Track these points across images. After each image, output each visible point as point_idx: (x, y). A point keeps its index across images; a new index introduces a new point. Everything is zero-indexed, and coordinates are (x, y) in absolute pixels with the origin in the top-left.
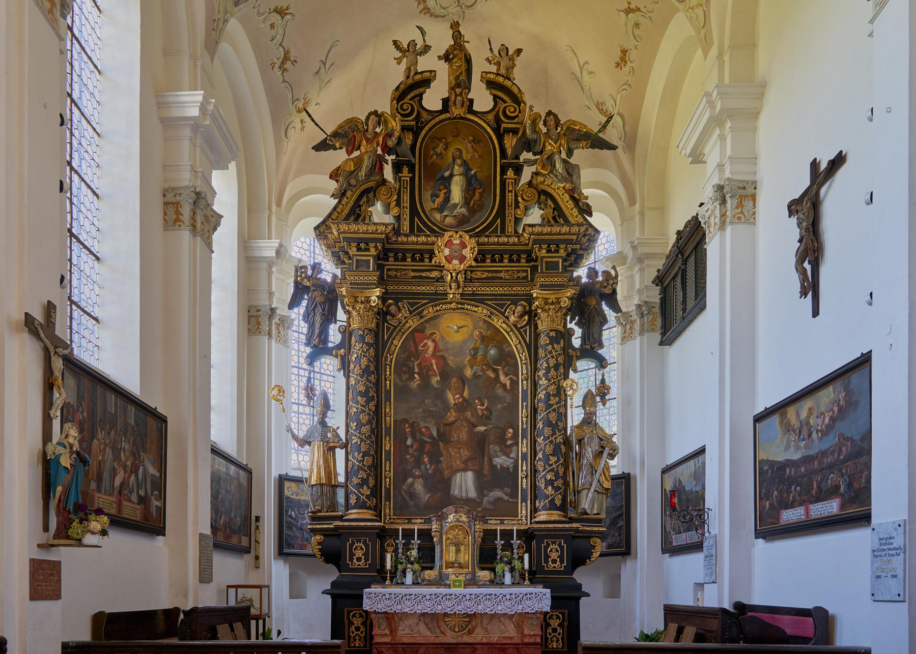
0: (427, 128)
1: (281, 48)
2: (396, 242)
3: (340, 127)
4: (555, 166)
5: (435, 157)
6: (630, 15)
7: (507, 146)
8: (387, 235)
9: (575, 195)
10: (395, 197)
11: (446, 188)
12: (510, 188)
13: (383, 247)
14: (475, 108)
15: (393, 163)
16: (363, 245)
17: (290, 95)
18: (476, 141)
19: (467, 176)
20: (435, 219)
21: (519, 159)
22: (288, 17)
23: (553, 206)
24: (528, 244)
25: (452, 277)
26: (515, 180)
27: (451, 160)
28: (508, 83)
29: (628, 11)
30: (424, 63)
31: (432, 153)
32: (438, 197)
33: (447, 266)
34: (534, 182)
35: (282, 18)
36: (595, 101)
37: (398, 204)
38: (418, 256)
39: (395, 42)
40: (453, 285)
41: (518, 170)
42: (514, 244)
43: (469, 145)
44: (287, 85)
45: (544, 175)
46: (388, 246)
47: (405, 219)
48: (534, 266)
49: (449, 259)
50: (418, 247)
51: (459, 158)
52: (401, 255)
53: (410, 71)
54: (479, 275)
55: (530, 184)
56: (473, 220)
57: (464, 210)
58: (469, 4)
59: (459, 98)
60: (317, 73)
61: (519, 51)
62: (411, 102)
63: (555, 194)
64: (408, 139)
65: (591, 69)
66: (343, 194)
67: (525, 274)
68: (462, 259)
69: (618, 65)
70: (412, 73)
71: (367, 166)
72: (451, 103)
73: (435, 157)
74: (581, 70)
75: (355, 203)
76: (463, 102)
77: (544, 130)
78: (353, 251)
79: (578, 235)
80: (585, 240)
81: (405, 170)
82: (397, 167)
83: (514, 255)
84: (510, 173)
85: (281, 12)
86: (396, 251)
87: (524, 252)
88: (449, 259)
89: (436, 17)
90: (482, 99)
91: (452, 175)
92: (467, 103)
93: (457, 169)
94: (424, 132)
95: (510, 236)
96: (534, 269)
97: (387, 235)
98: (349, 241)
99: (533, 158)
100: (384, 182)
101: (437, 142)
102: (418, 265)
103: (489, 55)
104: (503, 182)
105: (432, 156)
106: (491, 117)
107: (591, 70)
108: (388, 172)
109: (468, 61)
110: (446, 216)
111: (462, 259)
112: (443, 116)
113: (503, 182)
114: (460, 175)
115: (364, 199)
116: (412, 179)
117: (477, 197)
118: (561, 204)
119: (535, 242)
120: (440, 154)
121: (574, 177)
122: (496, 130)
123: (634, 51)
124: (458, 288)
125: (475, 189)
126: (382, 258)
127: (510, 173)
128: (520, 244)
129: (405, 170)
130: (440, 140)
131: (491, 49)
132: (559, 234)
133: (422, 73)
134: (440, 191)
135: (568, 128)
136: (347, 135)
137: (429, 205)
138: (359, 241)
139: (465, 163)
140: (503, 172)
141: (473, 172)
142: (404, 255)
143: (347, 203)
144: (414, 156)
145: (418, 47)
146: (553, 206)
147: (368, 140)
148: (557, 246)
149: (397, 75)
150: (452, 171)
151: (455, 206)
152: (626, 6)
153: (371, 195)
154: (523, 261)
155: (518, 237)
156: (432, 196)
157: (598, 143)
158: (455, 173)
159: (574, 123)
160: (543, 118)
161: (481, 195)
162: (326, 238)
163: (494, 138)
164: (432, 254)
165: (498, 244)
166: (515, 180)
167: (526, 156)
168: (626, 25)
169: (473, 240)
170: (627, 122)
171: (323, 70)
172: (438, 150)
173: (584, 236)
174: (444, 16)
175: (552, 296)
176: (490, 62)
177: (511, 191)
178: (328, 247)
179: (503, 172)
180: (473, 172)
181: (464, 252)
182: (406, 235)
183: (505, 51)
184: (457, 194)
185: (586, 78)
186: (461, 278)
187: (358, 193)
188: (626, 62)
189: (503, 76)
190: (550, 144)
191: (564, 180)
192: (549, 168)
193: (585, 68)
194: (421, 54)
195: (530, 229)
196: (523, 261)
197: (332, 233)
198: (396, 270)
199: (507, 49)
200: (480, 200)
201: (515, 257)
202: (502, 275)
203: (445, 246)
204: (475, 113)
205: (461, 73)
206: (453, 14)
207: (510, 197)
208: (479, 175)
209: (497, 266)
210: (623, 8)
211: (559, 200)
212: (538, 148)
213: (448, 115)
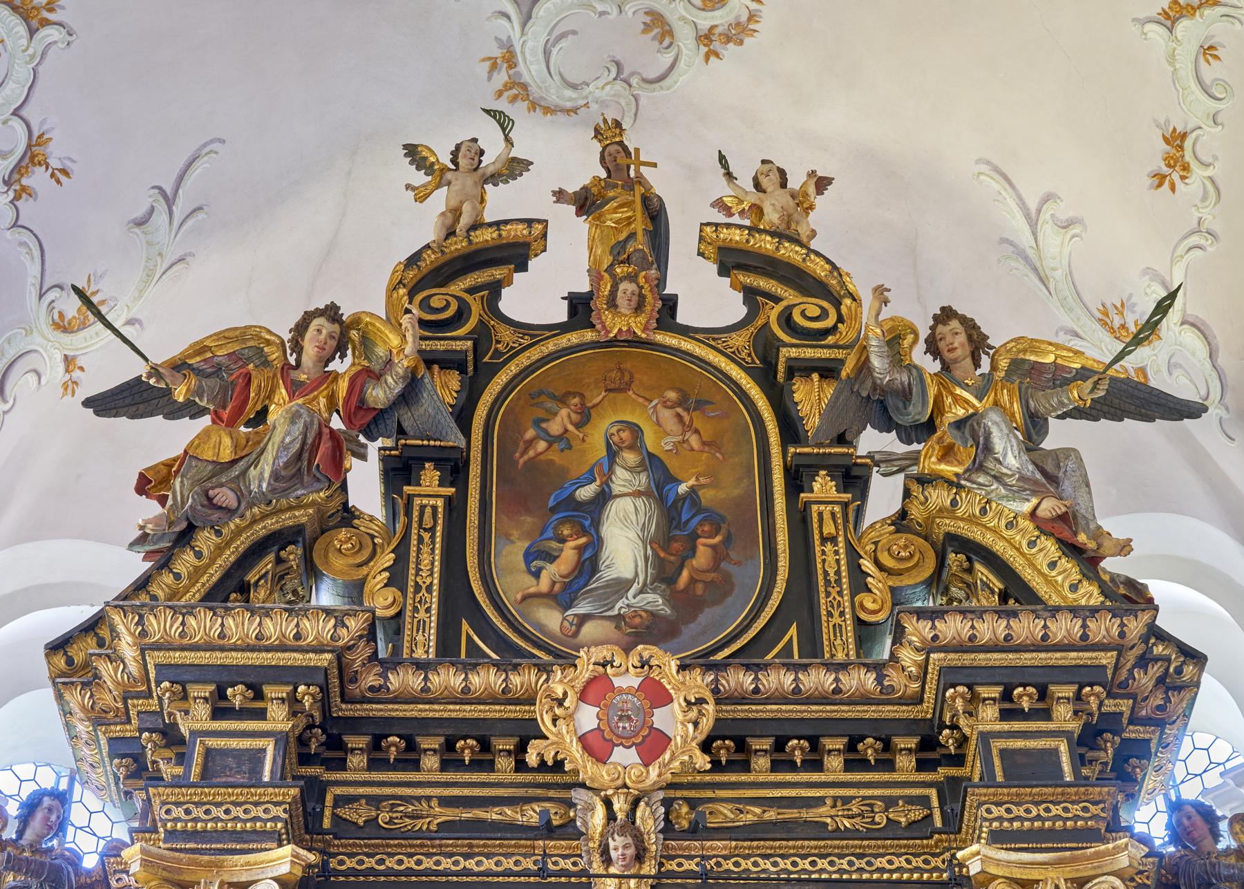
0: (512, 368)
1: (17, 124)
2: (378, 694)
3: (200, 348)
4: (988, 449)
5: (542, 445)
6: (1183, 26)
7: (804, 409)
8: (340, 655)
9: (1082, 538)
10: (387, 559)
11: (583, 531)
12: (829, 529)
13: (324, 703)
14: (682, 318)
15: (384, 459)
16: (237, 695)
17: (35, 270)
18: (690, 402)
19: (661, 499)
20: (541, 627)
21: (850, 444)
23: (998, 585)
24: (918, 699)
25: (611, 816)
26: (845, 505)
27: (603, 452)
28: (790, 252)
30: (503, 203)
31: (530, 434)
32: (551, 558)
33: (589, 770)
34: (916, 512)
36: (1095, 306)
37: (397, 577)
38: (467, 748)
39: (412, 151)
40: (618, 844)
41: (853, 479)
42: (865, 699)
43: (667, 415)
44: (26, 237)
45: (953, 484)
46: (347, 710)
47: (421, 626)
48: (954, 781)
49: (597, 747)
50: (469, 711)
51: (631, 448)
52: (396, 743)
53: (457, 219)
54: (725, 814)
55: (901, 521)
56: (689, 631)
57: (655, 601)
58: (653, 75)
59: (624, 286)
60: (141, 223)
61: (822, 184)
62: (466, 296)
63: (999, 547)
64: (445, 388)
65: (1063, 210)
66: (185, 537)
67: (917, 814)
68: (653, 745)
69: (1160, 179)
70: (465, 220)
71: (284, 447)
72: (599, 303)
73: (542, 445)
74: (1033, 225)
75: (227, 575)
76: (642, 298)
77: (931, 366)
78: (195, 718)
79: (1120, 650)
80: (1145, 680)
81: (430, 477)
82: (399, 472)
83: (866, 744)
84: (823, 487)
86: (378, 732)
87: (908, 727)
88: (597, 747)
89: (548, 110)
90: (707, 298)
91: (604, 497)
92: (653, 304)
93: (622, 479)
94: (502, 378)
95: (844, 666)
96: (953, 792)
97: (340, 655)
98: (181, 678)
99: (901, 448)
100: (348, 515)
101: (550, 404)
102: (468, 783)
103: (722, 189)
104: (800, 521)
105: (530, 443)
106: (740, 340)
107: (1063, 216)
108: (365, 484)
109: (655, 214)
110: (583, 619)
111: (653, 745)
112: (574, 338)
113: (800, 521)
114: (637, 494)
115: (267, 564)
116: (455, 508)
117: (702, 557)
118: (1027, 574)
119: (950, 676)
120: (563, 437)
121: (1067, 486)
122: (765, 374)
123: (1210, 129)
124: (639, 858)
125: (694, 537)
126: (321, 744)
127: (823, 487)
128: (886, 696)
129: (430, 477)
130: (563, 400)
131: (729, 175)
132: (1044, 645)
133: (498, 224)
134: (563, 540)
135: (1016, 364)
136: (226, 378)
137: (514, 581)
138: (222, 679)
139: (652, 463)
140: (797, 479)
141: (683, 488)
142: (411, 746)
143: (197, 573)
144: (467, 432)
145: (486, 160)
146: (998, 585)
147: (295, 389)
148: (1043, 694)
149: (419, 226)
150: (607, 483)
151: (621, 586)
153: (293, 554)
154: (905, 762)
155: (878, 668)
156: (529, 556)
157: (1133, 401)
158: (617, 488)
159: (1033, 345)
160: (924, 333)
161: (719, 554)
162: (92, 681)
163: (755, 392)
164: (528, 732)
165: (796, 696)
166: (845, 505)
167: (871, 441)
168: (1172, 58)
169: (699, 682)
170: (1220, 340)
171: (161, 218)
172: (555, 427)
173: (1144, 661)
174: (575, 110)
175: (1052, 874)
176: (728, 211)
177: (833, 539)
178: (98, 718)
179: (797, 479)
180: (683, 488)
181: (662, 718)
182: (422, 666)
183: (775, 176)
184: (624, 543)
185: (1054, 245)
186: (648, 819)
187: (242, 543)
188: (1186, 168)
189: (773, 234)
190: (957, 400)
191: (1027, 486)
192: (967, 453)
193: (1046, 215)
194: (495, 178)
195: (925, 628)
196: (905, 762)
197: (115, 658)
198: (375, 801)
199: (782, 173)
200: (715, 567)
201: (869, 750)
202: (823, 813)
203: (583, 697)
204: (686, 331)
205: (632, 236)
206: (603, 103)
207: (829, 559)
208: (706, 496)
209: (797, 784)
210: (1154, 11)
211: (1018, 564)
212: (918, 413)
213: (589, 335)
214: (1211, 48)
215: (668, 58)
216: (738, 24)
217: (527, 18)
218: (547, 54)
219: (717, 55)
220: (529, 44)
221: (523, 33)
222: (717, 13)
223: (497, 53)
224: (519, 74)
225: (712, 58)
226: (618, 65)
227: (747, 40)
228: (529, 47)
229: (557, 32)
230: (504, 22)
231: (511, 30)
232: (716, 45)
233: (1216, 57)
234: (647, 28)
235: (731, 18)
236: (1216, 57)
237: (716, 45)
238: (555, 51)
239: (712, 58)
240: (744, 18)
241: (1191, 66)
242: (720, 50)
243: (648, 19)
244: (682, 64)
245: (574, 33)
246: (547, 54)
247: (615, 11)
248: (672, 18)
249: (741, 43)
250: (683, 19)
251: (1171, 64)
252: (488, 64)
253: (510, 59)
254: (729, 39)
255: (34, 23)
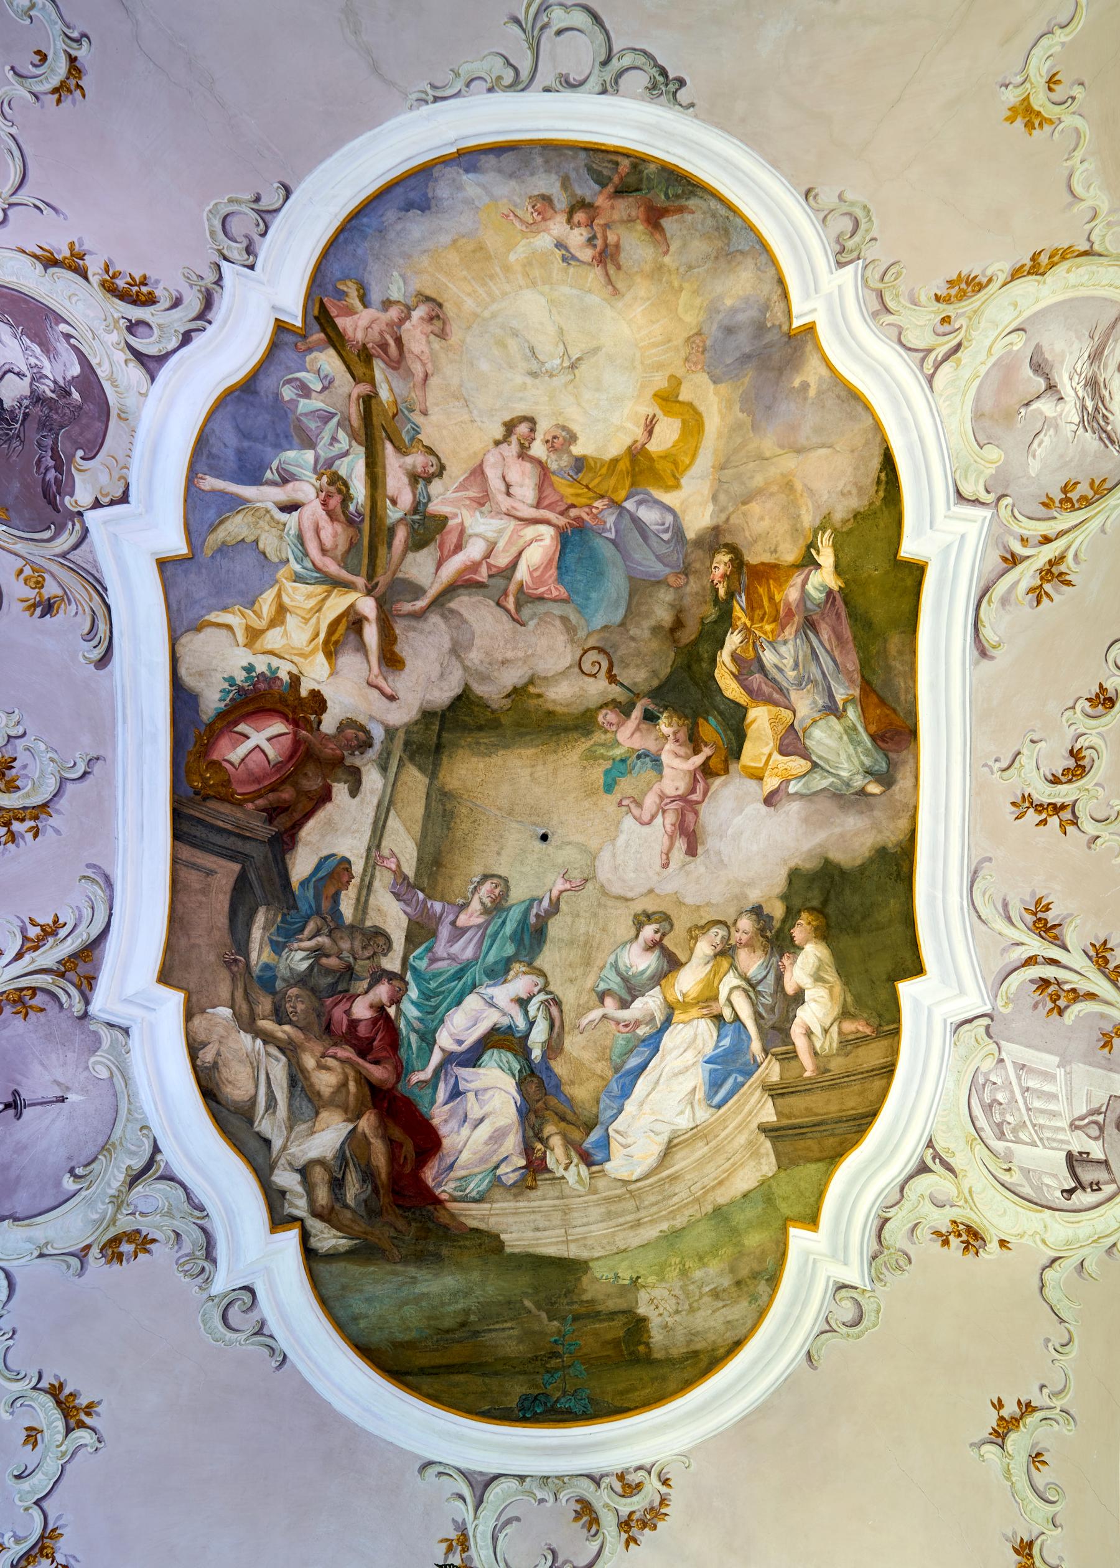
6: (1012, 1437)
22: (83, 1436)
29: (1000, 1435)
35: (69, 1430)
85: (73, 1412)
152: (991, 1419)
210: (985, 1433)
214: (1038, 1454)
215: (595, 1546)
216: (652, 1509)
217: (479, 1502)
218: (495, 1539)
219: (635, 1541)
220: (481, 1528)
221: (475, 1518)
222: (635, 1499)
223: (453, 1535)
224: (470, 1558)
225: (632, 1545)
226: (554, 1552)
227: (660, 1525)
228: (481, 1530)
229: (503, 1519)
230: (459, 1504)
231: (464, 1511)
232: (635, 1532)
233: (1044, 1463)
234: (578, 1515)
235: (645, 1504)
236: (1044, 1463)
237: (635, 1532)
238: (501, 1536)
239: (632, 1545)
240: (656, 1503)
241: (1025, 1477)
242: (638, 1537)
243: (578, 1507)
244: (606, 1552)
245: (518, 1519)
246: (495, 1539)
247: (552, 1499)
248: (597, 1505)
249: (655, 1528)
250: (606, 1506)
251: (1008, 1479)
252: (445, 1545)
253: (463, 1542)
254: (644, 1524)
255: (72, 1422)
